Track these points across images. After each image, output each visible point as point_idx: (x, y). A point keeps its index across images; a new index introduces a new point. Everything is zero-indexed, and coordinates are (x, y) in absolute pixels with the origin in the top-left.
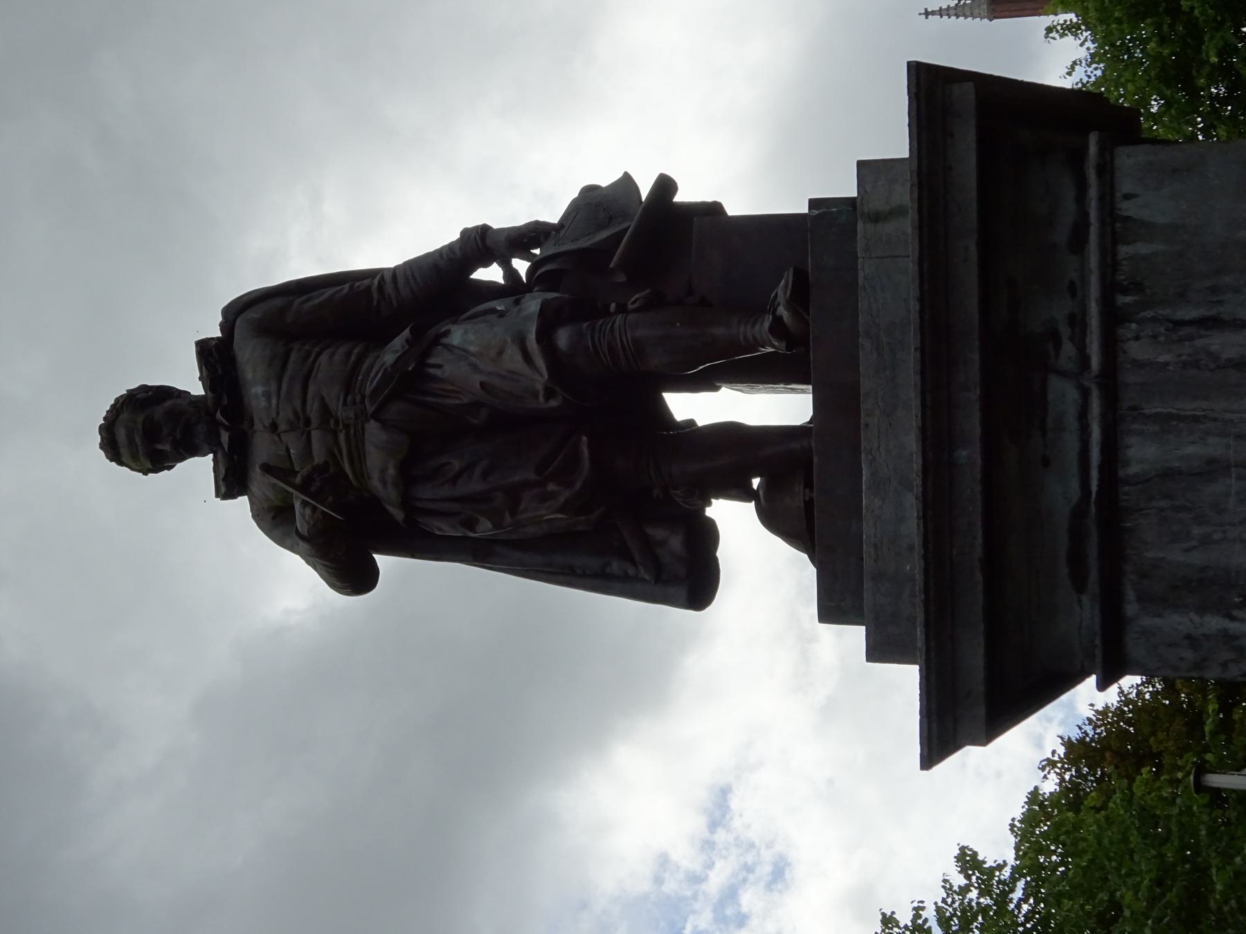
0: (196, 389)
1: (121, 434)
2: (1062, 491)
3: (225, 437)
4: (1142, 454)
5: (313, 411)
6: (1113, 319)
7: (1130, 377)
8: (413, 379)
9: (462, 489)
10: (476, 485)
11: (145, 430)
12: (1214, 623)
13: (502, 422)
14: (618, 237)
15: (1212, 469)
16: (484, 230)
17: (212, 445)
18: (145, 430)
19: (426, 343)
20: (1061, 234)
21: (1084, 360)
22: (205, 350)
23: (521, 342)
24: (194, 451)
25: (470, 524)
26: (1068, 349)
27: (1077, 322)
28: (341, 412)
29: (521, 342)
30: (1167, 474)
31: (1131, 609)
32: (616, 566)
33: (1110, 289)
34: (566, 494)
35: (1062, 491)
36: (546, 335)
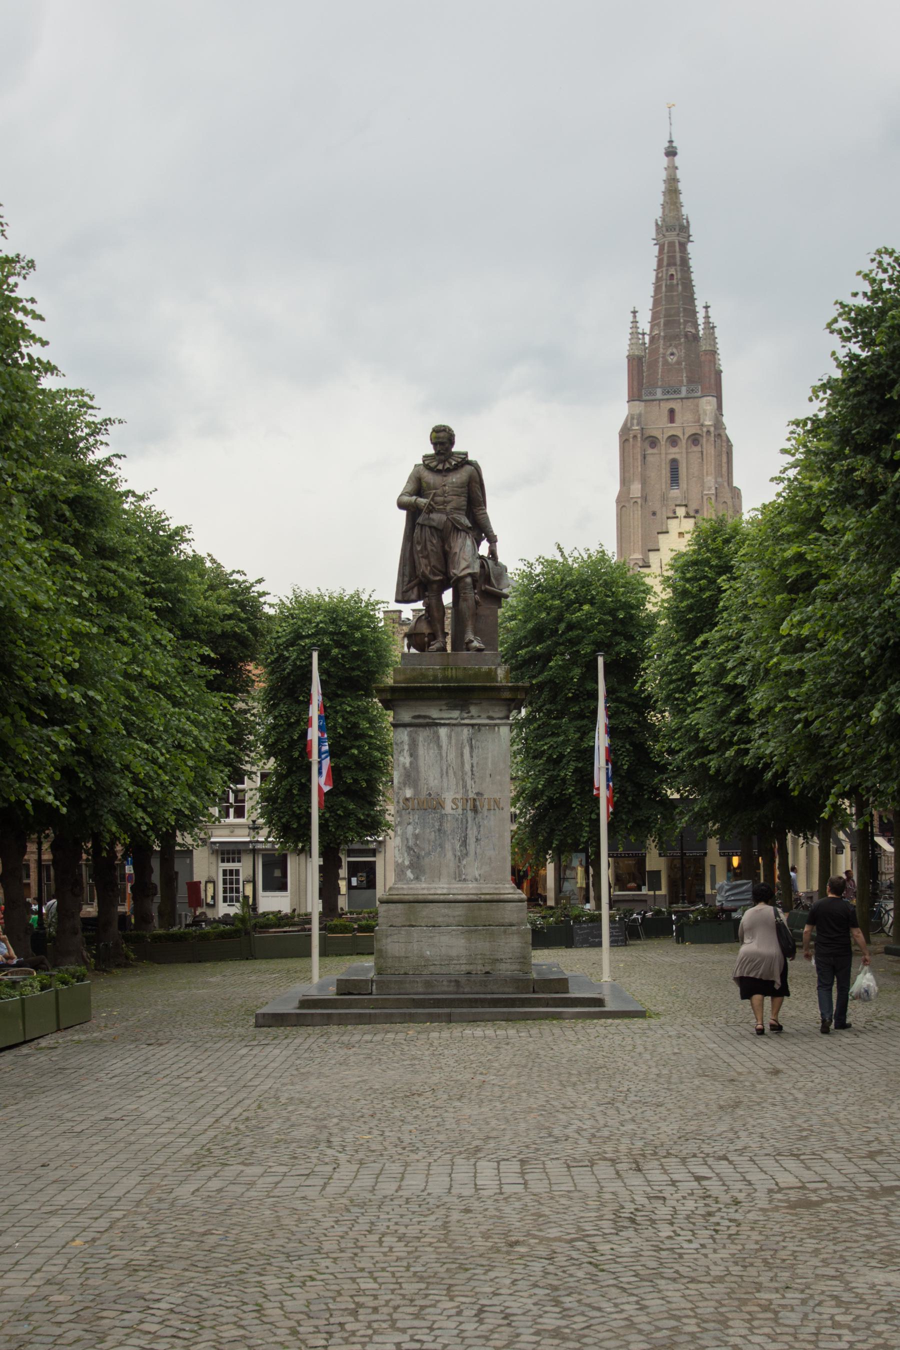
0: (453, 450)
1: (442, 434)
2: (434, 713)
3: (440, 467)
4: (443, 731)
5: (449, 498)
6: (473, 725)
7: (460, 728)
8: (457, 528)
9: (428, 543)
10: (429, 547)
11: (443, 438)
12: (406, 747)
13: (446, 557)
14: (493, 586)
15: (440, 747)
16: (496, 541)
17: (438, 453)
18: (443, 438)
19: (467, 530)
20: (491, 714)
21: (463, 719)
22: (466, 454)
23: (468, 567)
24: (435, 449)
25: (418, 543)
26: (466, 715)
27: (472, 717)
28: (448, 508)
29: (468, 567)
30: (438, 737)
31: (409, 729)
32: (406, 579)
33: (479, 725)
34: (427, 572)
35: (434, 713)
36: (470, 574)
